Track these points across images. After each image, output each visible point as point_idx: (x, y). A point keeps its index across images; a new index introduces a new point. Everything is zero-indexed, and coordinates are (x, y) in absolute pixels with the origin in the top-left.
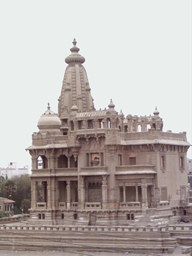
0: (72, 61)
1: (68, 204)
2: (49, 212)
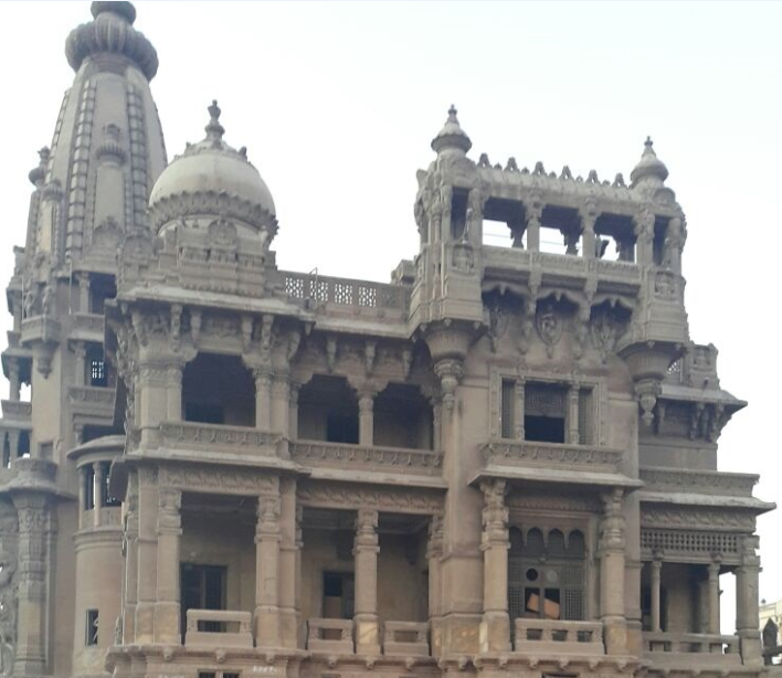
0: (121, 47)
1: (368, 631)
2: (277, 660)
